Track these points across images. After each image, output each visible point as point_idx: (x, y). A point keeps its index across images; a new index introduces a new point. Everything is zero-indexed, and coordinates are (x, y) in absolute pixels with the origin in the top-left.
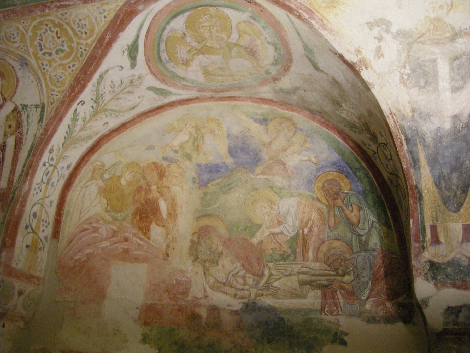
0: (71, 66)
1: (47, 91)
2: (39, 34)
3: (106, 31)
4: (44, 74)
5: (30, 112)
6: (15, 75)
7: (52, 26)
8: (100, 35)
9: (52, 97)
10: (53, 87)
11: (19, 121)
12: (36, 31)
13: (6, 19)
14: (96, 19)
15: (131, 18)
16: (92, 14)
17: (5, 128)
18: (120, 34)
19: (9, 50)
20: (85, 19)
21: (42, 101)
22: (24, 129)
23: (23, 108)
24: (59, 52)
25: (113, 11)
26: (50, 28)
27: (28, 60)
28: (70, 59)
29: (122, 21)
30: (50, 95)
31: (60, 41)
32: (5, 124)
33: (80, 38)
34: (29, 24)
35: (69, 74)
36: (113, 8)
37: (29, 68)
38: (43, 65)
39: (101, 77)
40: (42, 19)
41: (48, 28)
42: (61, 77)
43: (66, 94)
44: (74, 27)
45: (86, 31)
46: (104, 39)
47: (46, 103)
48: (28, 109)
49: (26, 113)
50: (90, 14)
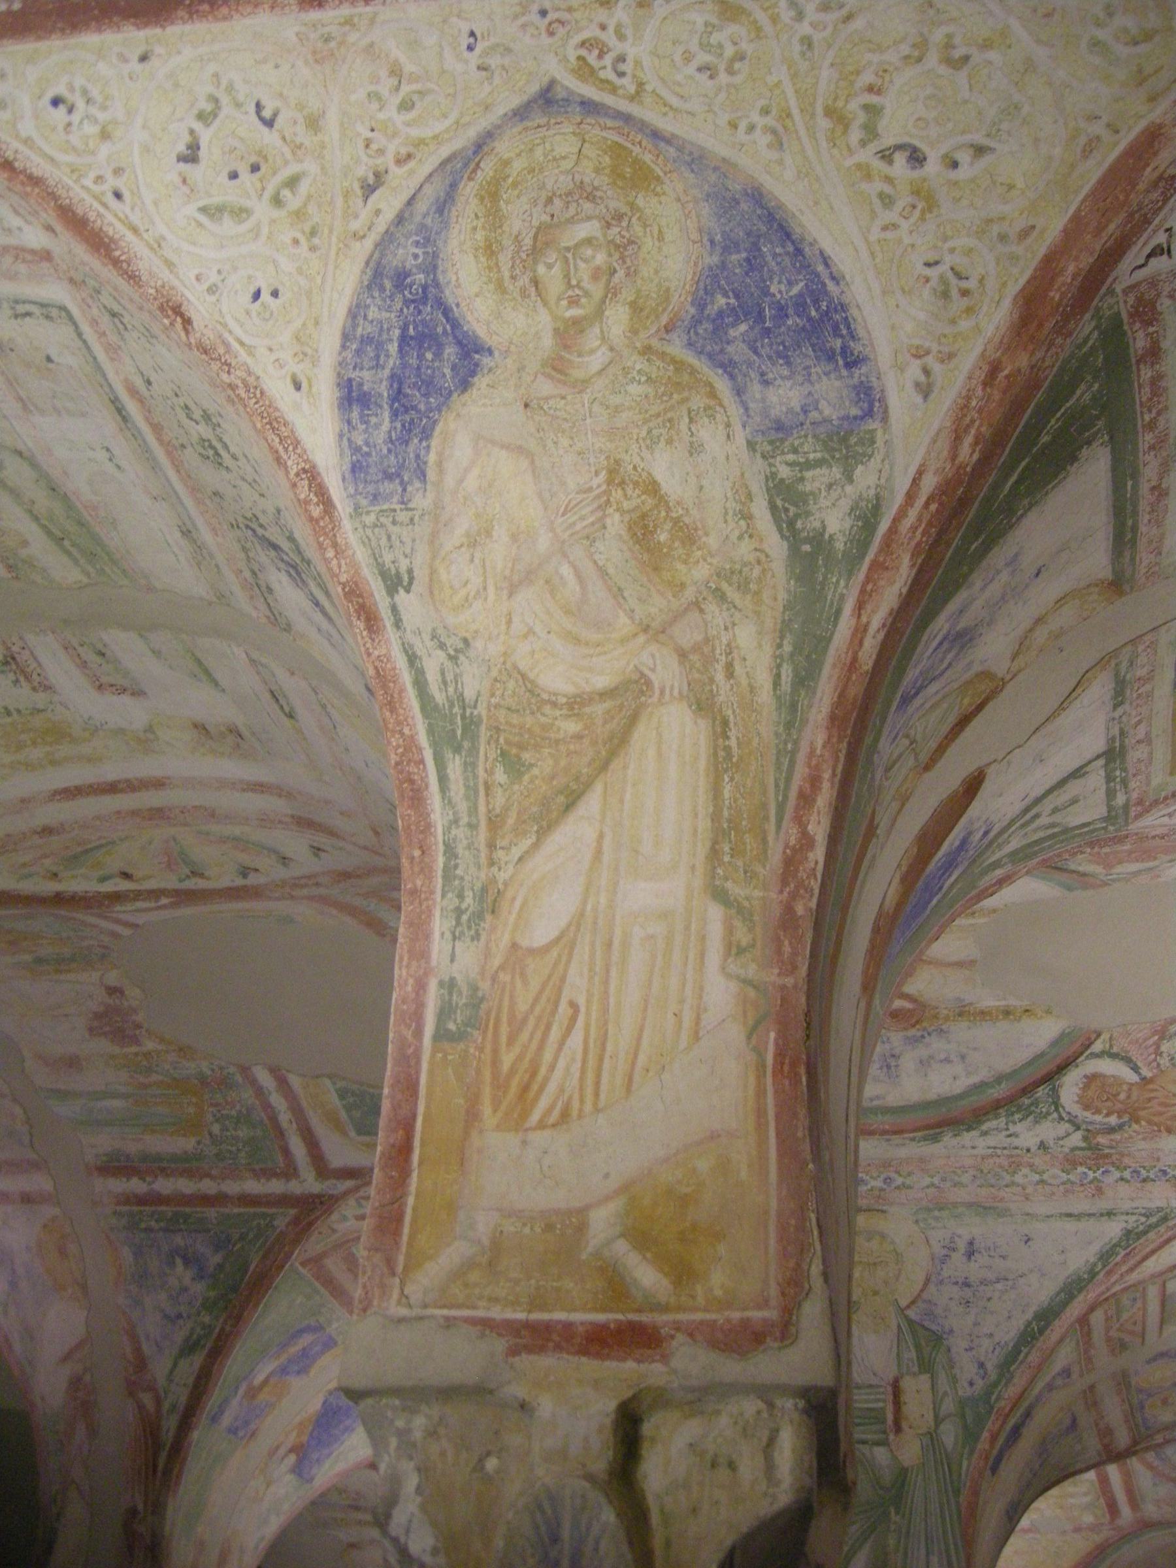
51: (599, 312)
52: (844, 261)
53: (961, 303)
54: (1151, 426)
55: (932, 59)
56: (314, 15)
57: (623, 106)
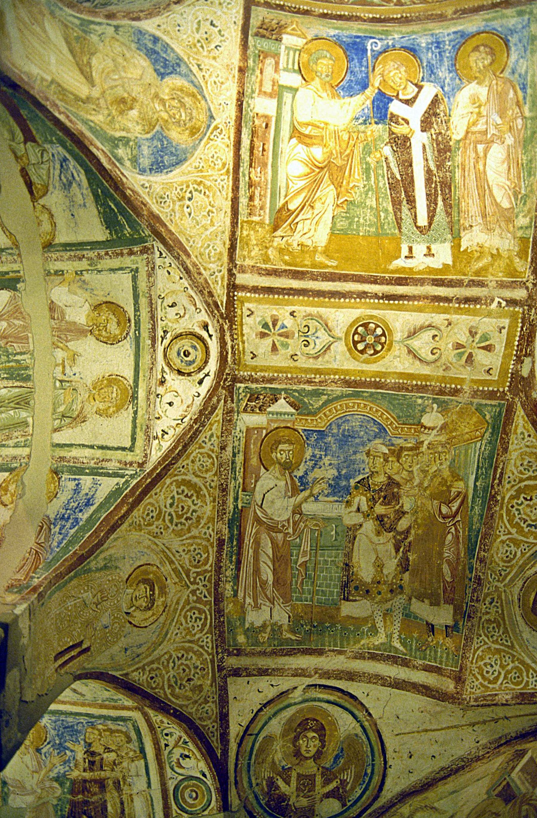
7: (516, 501)
14: (528, 446)
16: (521, 448)
26: (517, 504)
40: (505, 508)
41: (516, 507)
51: (167, 112)
52: (171, 175)
53: (159, 200)
54: (107, 254)
55: (210, 208)
56: (237, 69)
57: (208, 134)
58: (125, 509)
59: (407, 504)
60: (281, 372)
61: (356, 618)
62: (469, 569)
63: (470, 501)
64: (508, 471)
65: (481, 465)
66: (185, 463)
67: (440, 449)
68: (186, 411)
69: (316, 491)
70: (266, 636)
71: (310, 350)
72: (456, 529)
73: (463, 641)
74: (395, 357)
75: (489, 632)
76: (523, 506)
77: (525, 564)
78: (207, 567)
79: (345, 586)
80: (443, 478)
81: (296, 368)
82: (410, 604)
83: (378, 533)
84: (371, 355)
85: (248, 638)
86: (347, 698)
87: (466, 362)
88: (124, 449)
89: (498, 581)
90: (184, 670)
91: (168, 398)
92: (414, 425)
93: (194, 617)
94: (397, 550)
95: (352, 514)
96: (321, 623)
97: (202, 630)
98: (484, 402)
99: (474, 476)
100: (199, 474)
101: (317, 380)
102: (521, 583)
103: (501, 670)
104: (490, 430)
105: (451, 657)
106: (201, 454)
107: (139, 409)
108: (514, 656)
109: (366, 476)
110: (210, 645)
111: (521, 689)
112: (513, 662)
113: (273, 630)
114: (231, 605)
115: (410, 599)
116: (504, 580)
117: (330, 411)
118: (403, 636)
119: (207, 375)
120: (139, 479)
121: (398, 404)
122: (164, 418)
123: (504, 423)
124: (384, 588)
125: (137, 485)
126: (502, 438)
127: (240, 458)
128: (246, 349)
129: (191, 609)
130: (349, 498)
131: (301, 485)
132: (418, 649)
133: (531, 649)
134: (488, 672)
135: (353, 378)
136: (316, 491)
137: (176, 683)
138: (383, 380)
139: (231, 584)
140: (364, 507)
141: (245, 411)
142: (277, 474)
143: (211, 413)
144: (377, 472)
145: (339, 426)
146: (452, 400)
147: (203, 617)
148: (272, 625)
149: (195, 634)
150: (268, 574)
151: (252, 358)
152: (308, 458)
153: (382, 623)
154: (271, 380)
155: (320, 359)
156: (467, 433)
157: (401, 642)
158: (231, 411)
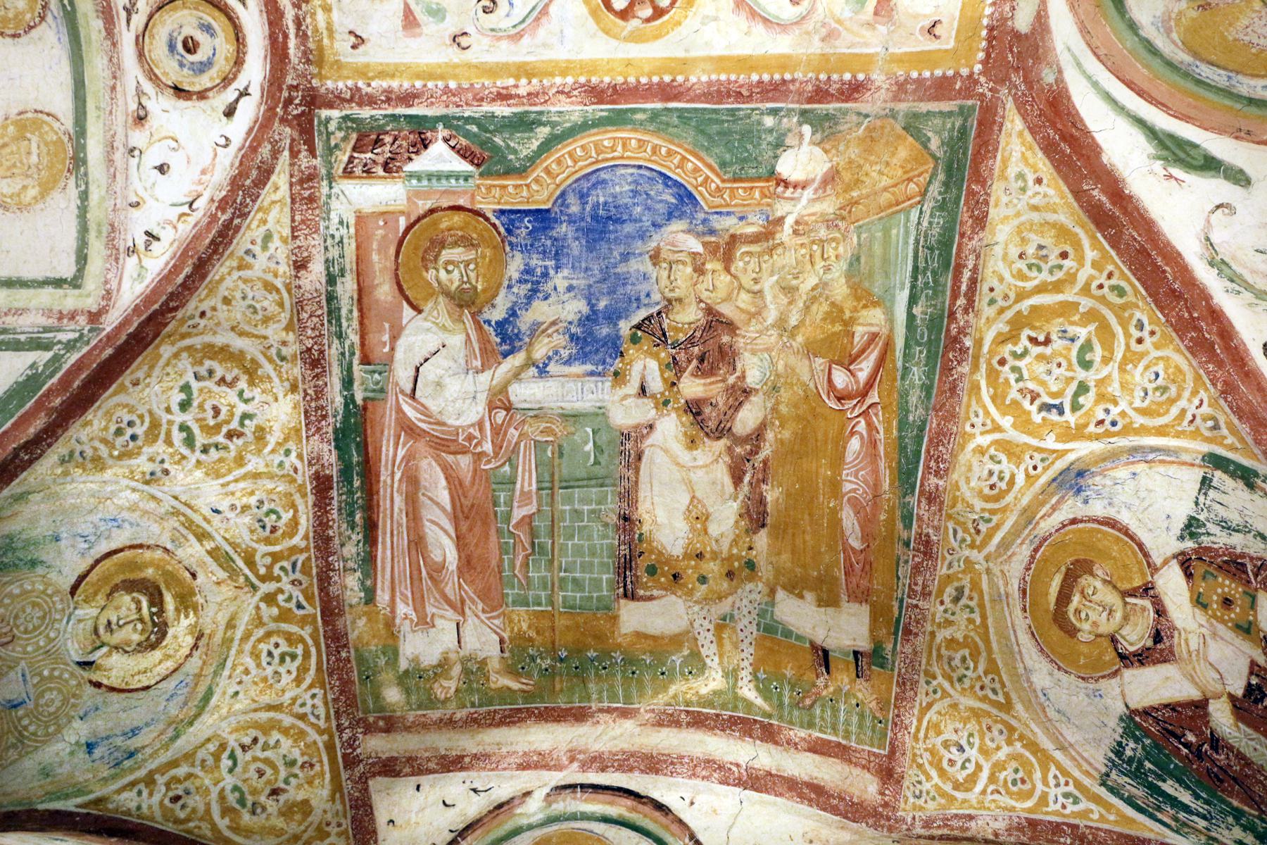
0: (1136, 334)
1: (1178, 435)
2: (1019, 397)
3: (1078, 194)
4: (1128, 430)
5: (1212, 516)
6: (1095, 526)
7: (1009, 347)
8: (1085, 219)
9: (1198, 420)
10: (1174, 411)
11: (1225, 562)
12: (1007, 402)
13: (947, 470)
14: (1035, 208)
15: (1069, 114)
16: (1018, 214)
17: (1223, 622)
18: (1105, 159)
19: (1025, 510)
20: (1024, 241)
21: (1198, 462)
22: (1252, 552)
23: (1193, 535)
24: (1088, 357)
25: (1029, 154)
26: (1014, 354)
27: (1072, 464)
28: (1118, 330)
29: (1066, 138)
30: (1192, 428)
31: (1060, 341)
32: (1214, 616)
33: (1071, 278)
34: (981, 413)
35: (1157, 346)
36: (1023, 149)
37: (1093, 469)
38: (1101, 422)
39: (1219, 264)
40: (983, 367)
41: (1011, 362)
42: (1157, 375)
43: (1208, 373)
44: (1036, 282)
45: (1057, 252)
46: (1100, 205)
47: (1206, 448)
48: (1202, 517)
49: (1211, 528)
50: (1016, 222)
58: (39, 423)
59: (753, 370)
60: (431, 76)
61: (654, 638)
62: (904, 518)
63: (899, 354)
64: (988, 272)
65: (922, 265)
66: (205, 306)
67: (823, 233)
68: (200, 183)
69: (540, 352)
70: (452, 685)
71: (499, 19)
72: (870, 425)
73: (895, 689)
74: (706, 20)
75: (953, 670)
76: (1028, 359)
77: (1038, 502)
78: (297, 540)
79: (625, 566)
80: (833, 304)
81: (469, 66)
82: (773, 604)
83: (692, 443)
84: (648, 20)
85: (408, 692)
86: (647, 809)
87: (876, 13)
88: (58, 283)
89: (972, 546)
90: (261, 773)
91: (154, 156)
92: (759, 179)
93: (276, 653)
94: (737, 479)
95: (630, 400)
96: (578, 650)
97: (298, 681)
98: (924, 107)
99: (907, 292)
100: (247, 328)
101: (522, 91)
102: (1025, 552)
103: (982, 761)
104: (941, 177)
105: (868, 723)
106: (245, 281)
107: (92, 188)
108: (1011, 729)
109: (654, 310)
110: (321, 711)
111: (1030, 810)
112: (1009, 742)
113: (466, 672)
114: (361, 623)
115: (772, 592)
116: (985, 543)
117: (559, 162)
118: (762, 675)
119: (244, 93)
120: (85, 350)
121: (719, 133)
122: (150, 202)
123: (977, 153)
124: (712, 568)
125: (78, 366)
126: (971, 193)
127: (347, 288)
128: (336, 27)
129: (268, 635)
130: (618, 364)
131: (503, 341)
132: (796, 705)
133: (1051, 713)
134: (952, 762)
135: (607, 80)
136: (540, 352)
137: (242, 801)
138: (680, 79)
139: (358, 574)
140: (656, 385)
141: (348, 173)
142: (445, 320)
143: (262, 181)
144: (679, 300)
145: (583, 197)
146: (845, 113)
147: (300, 650)
148: (465, 661)
149: (283, 691)
150: (444, 548)
151: (354, 47)
152: (516, 276)
153: (714, 648)
154: (408, 98)
155: (526, 40)
156: (885, 189)
157: (757, 689)
158: (309, 178)
